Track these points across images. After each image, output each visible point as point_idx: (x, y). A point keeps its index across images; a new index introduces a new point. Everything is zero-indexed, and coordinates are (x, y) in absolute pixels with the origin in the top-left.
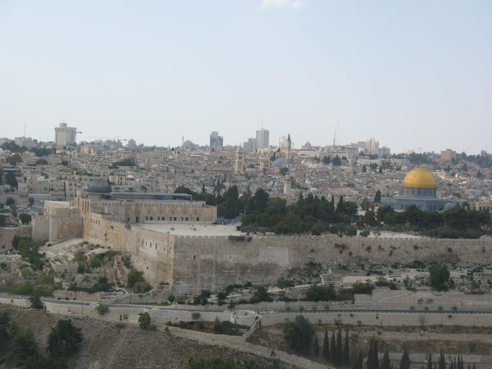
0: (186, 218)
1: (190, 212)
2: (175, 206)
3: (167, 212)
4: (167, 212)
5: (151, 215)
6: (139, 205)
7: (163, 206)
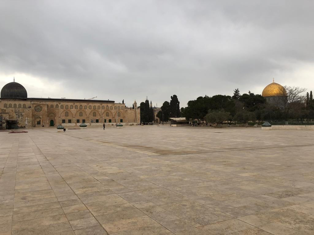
0: (109, 120)
1: (114, 114)
2: (97, 107)
3: (88, 115)
4: (88, 115)
5: (69, 118)
6: (54, 107)
7: (83, 108)
